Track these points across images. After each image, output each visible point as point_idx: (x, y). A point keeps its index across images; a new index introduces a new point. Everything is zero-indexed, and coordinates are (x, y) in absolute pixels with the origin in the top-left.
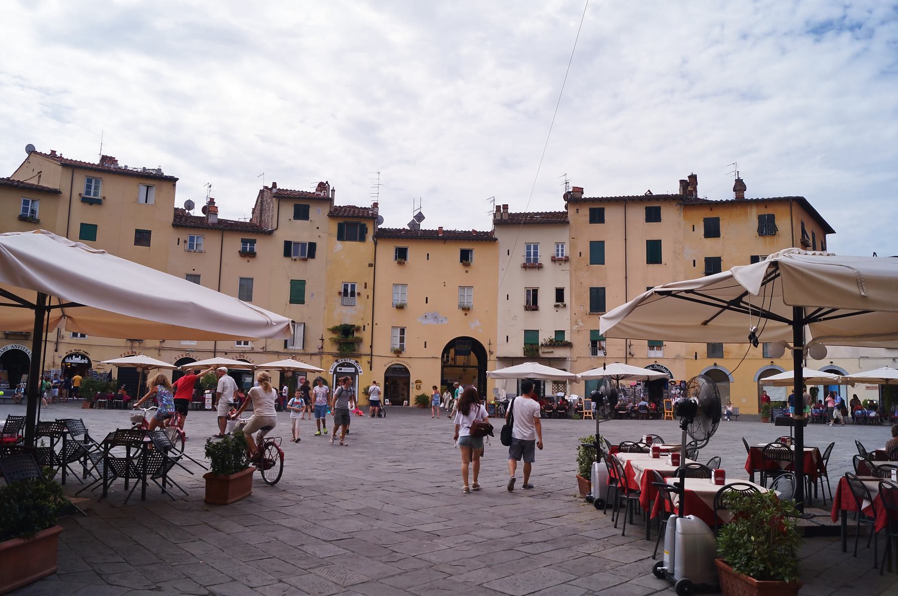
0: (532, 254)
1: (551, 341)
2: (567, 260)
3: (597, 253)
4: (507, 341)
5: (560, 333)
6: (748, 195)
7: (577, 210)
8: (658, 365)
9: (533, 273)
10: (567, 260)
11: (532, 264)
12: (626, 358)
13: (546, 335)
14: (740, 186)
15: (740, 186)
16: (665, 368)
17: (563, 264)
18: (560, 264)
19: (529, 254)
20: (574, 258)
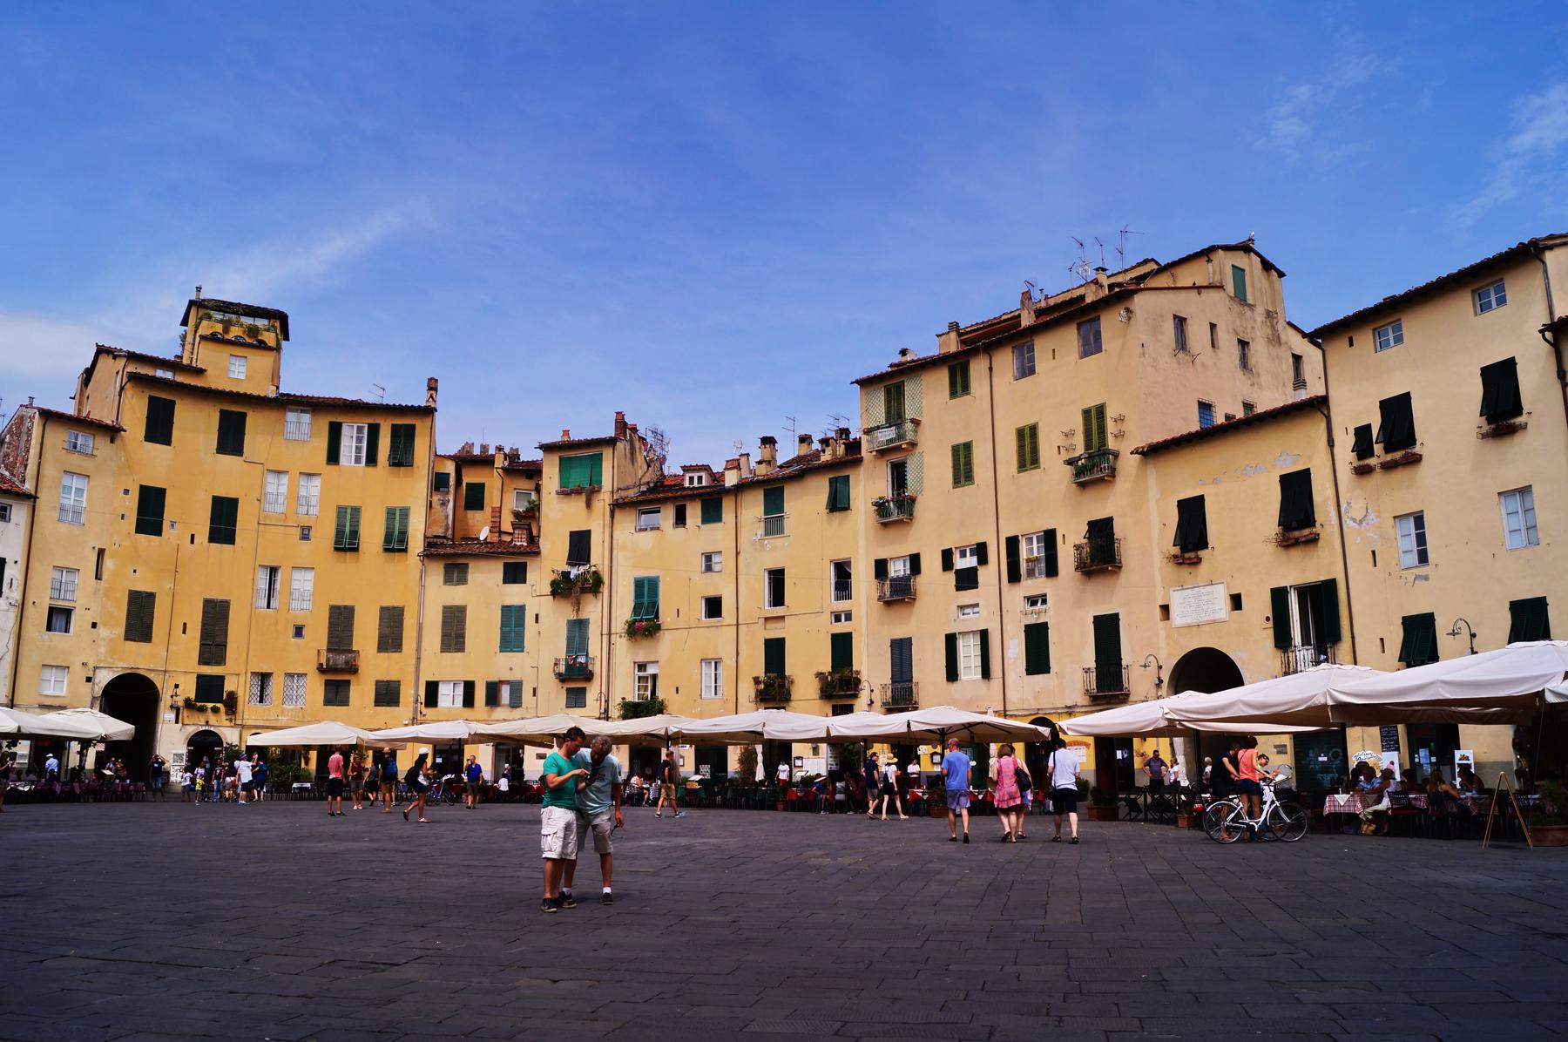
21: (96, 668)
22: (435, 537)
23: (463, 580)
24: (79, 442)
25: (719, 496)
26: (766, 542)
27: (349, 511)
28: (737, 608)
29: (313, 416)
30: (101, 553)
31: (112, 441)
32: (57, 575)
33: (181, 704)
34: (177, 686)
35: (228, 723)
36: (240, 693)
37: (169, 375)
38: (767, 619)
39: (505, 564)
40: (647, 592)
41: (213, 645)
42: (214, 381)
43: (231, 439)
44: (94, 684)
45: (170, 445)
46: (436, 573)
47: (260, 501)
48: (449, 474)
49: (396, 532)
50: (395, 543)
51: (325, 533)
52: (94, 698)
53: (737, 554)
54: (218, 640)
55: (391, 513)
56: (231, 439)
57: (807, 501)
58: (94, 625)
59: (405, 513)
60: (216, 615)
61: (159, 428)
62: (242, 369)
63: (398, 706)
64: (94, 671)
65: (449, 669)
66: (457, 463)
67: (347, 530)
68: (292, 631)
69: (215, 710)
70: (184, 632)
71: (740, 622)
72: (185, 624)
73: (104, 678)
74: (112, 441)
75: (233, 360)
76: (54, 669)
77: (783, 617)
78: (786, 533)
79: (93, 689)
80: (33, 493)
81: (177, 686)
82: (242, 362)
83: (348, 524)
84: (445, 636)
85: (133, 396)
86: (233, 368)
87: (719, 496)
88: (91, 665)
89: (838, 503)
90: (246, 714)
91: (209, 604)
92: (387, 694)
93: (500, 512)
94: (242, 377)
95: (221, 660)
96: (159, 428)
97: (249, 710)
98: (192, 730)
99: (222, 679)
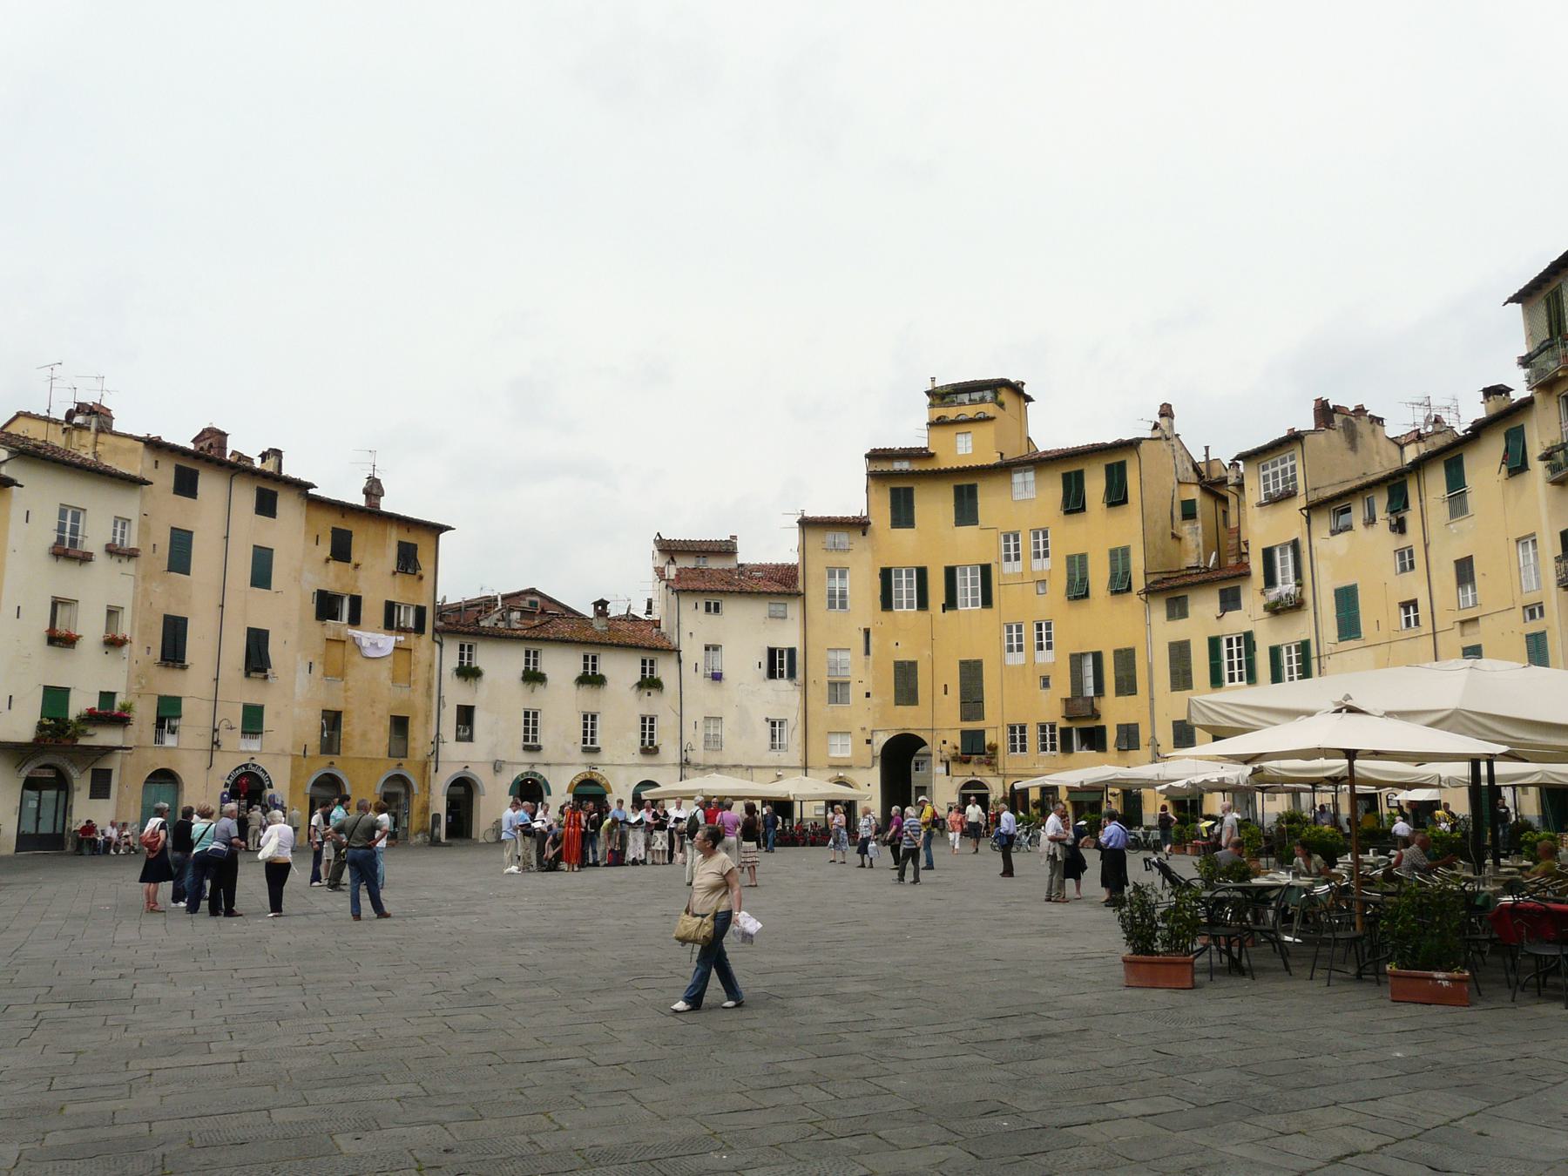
0: (68, 529)
1: (91, 711)
2: (132, 554)
3: (180, 553)
4: (10, 708)
5: (107, 697)
6: (386, 505)
7: (157, 462)
8: (254, 765)
9: (68, 570)
10: (132, 554)
11: (67, 551)
12: (212, 750)
13: (79, 705)
14: (374, 489)
15: (374, 489)
16: (263, 770)
17: (124, 560)
18: (120, 561)
19: (61, 528)
20: (145, 553)
21: (873, 731)
22: (1188, 568)
23: (1184, 615)
24: (837, 541)
25: (1401, 479)
26: (1452, 526)
27: (1077, 559)
28: (1432, 613)
29: (1036, 473)
30: (867, 632)
31: (864, 534)
32: (832, 656)
33: (948, 758)
34: (944, 742)
35: (991, 773)
36: (1000, 744)
37: (905, 466)
38: (1463, 623)
39: (1222, 592)
40: (1347, 599)
41: (972, 703)
42: (945, 463)
43: (966, 512)
44: (872, 747)
45: (913, 527)
46: (1159, 611)
47: (998, 563)
48: (1194, 500)
49: (1120, 573)
50: (1120, 585)
51: (1059, 582)
52: (874, 757)
53: (1426, 546)
54: (976, 698)
55: (1113, 553)
56: (966, 512)
57: (1483, 467)
58: (868, 695)
59: (1125, 552)
60: (971, 673)
61: (903, 515)
62: (970, 444)
63: (1139, 749)
64: (872, 734)
65: (1173, 705)
66: (1201, 486)
67: (1078, 580)
68: (1039, 683)
69: (980, 763)
70: (946, 693)
71: (1437, 630)
72: (946, 686)
73: (881, 739)
74: (864, 534)
75: (960, 438)
76: (839, 735)
77: (1475, 620)
78: (1470, 513)
79: (872, 750)
80: (803, 592)
81: (944, 742)
82: (969, 437)
83: (1077, 572)
84: (1173, 673)
85: (876, 490)
86: (959, 445)
87: (1401, 479)
88: (869, 729)
89: (1516, 465)
90: (1007, 763)
91: (965, 665)
92: (1129, 737)
93: (1239, 532)
94: (970, 451)
95: (980, 716)
96: (903, 515)
97: (1008, 760)
98: (960, 781)
99: (981, 733)
